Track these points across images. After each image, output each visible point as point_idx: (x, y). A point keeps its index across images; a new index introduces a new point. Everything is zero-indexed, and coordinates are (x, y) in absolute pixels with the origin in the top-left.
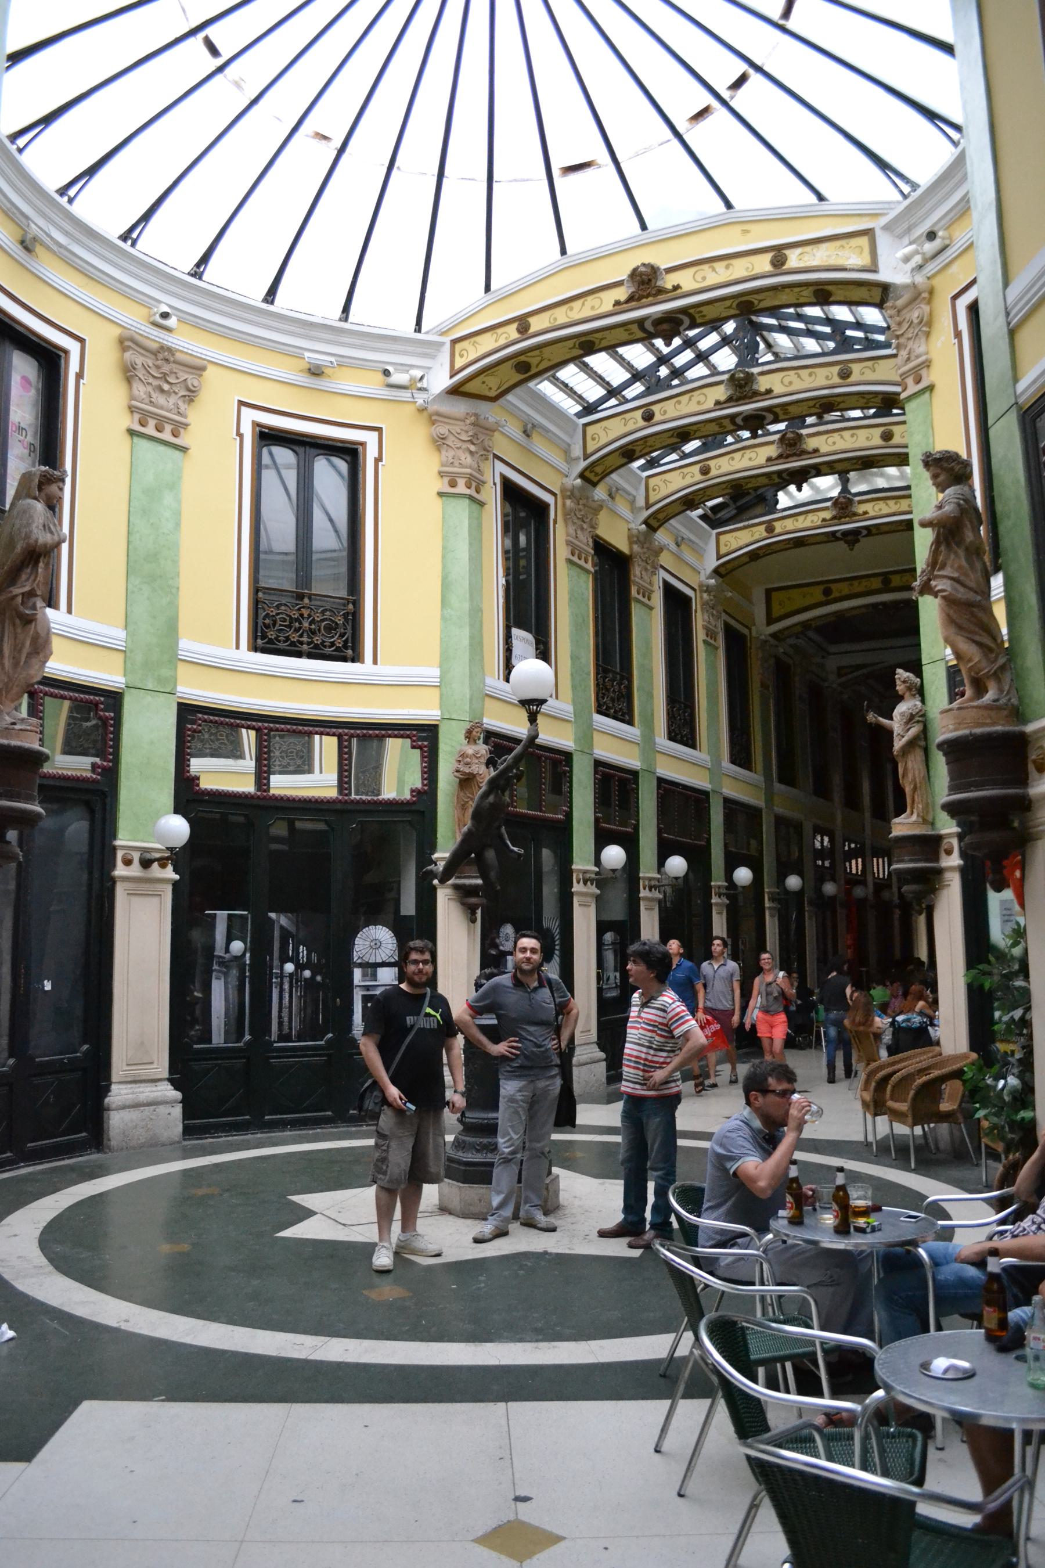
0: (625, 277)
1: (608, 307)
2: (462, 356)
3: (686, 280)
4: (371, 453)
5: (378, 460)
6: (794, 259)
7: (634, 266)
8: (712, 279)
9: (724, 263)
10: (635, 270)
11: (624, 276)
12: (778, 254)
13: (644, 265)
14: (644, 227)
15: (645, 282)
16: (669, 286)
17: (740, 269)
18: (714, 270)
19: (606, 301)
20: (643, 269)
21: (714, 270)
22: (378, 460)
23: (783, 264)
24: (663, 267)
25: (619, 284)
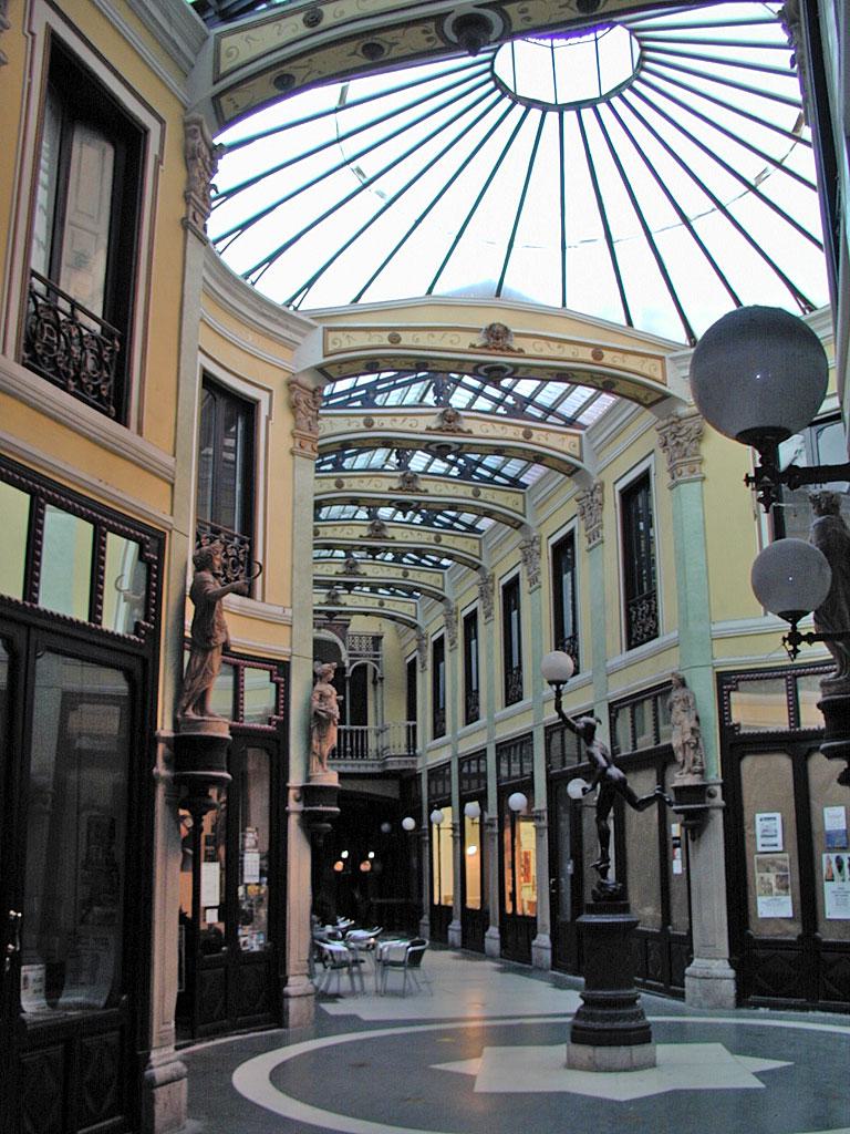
0: (484, 327)
1: (466, 347)
2: (334, 343)
3: (530, 347)
4: (263, 411)
5: (269, 418)
6: (608, 357)
7: (491, 322)
8: (546, 353)
9: (556, 344)
10: (492, 326)
11: (484, 325)
12: (598, 352)
13: (500, 325)
14: (498, 294)
15: (497, 336)
16: (516, 348)
17: (568, 351)
18: (549, 346)
19: (464, 341)
20: (496, 328)
21: (549, 346)
22: (269, 418)
23: (600, 359)
24: (513, 330)
25: (477, 331)
